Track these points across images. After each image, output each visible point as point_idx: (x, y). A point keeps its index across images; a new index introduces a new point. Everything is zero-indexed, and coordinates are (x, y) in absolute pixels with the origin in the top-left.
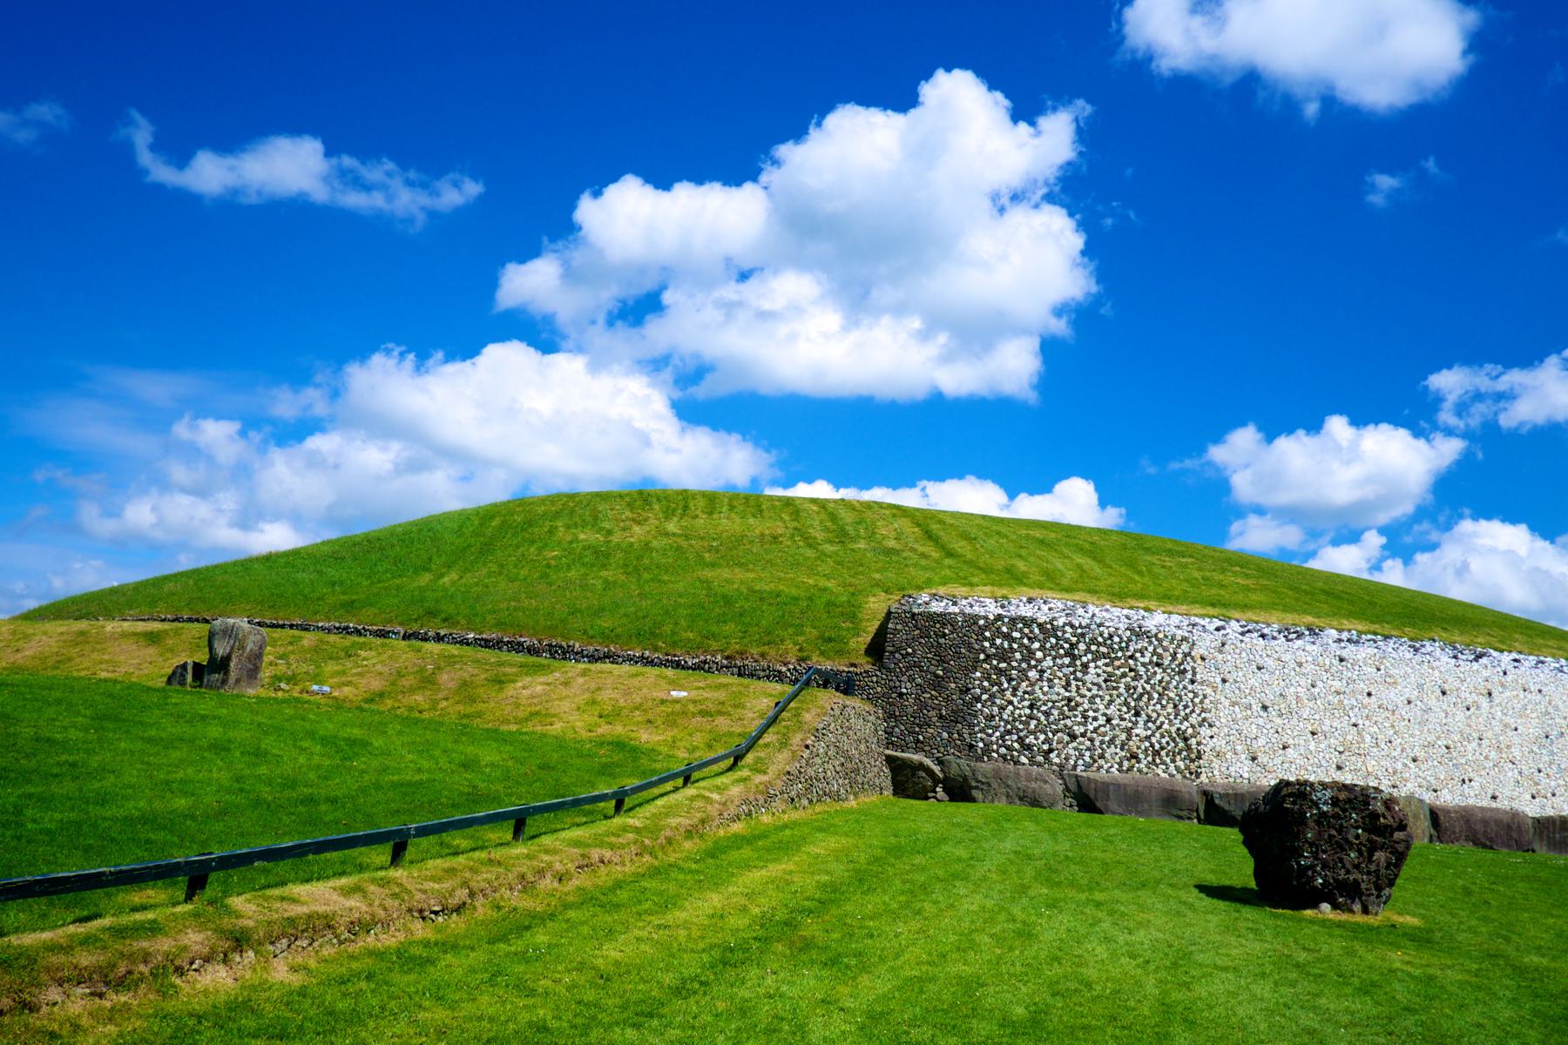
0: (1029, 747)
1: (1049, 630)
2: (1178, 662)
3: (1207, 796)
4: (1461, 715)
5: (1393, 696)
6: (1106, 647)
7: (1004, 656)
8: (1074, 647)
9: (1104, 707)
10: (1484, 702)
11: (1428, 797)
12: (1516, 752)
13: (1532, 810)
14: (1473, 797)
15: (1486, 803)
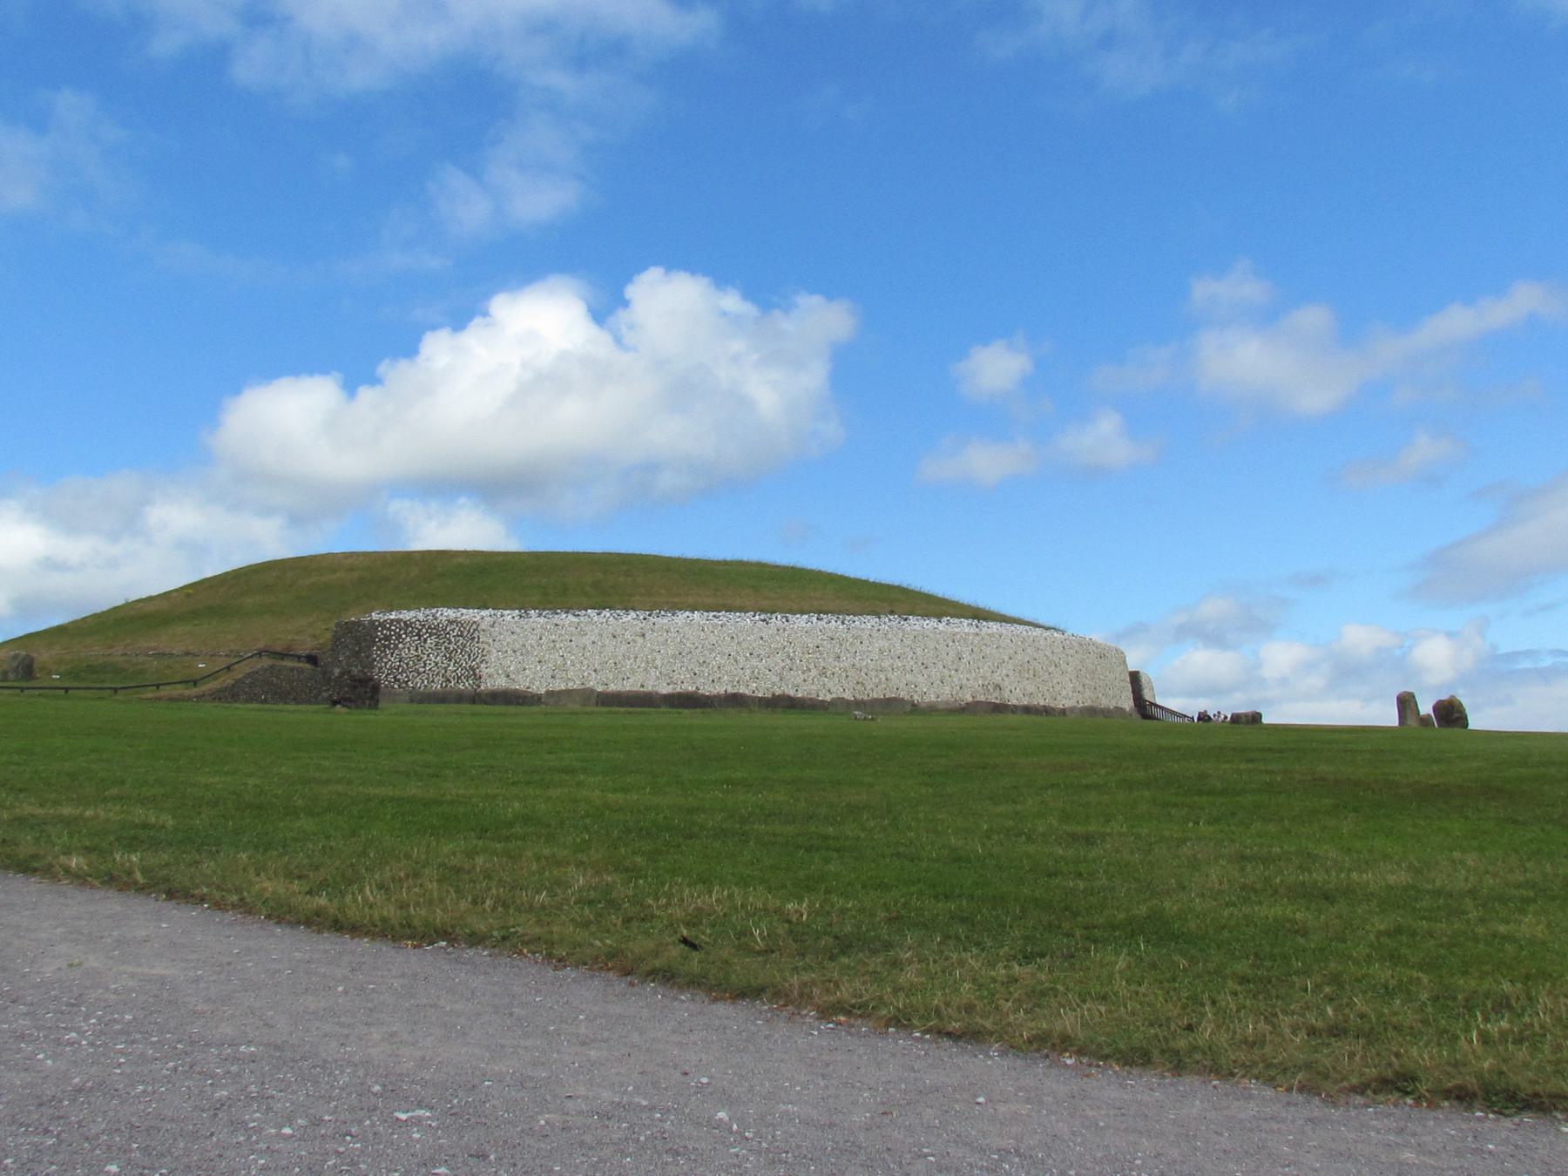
0: (396, 680)
1: (407, 624)
2: (469, 633)
3: (479, 695)
4: (624, 647)
5: (586, 640)
6: (437, 631)
7: (387, 638)
8: (417, 631)
9: (435, 658)
10: (640, 640)
11: (600, 689)
12: (658, 662)
13: (665, 689)
14: (629, 686)
15: (637, 688)
